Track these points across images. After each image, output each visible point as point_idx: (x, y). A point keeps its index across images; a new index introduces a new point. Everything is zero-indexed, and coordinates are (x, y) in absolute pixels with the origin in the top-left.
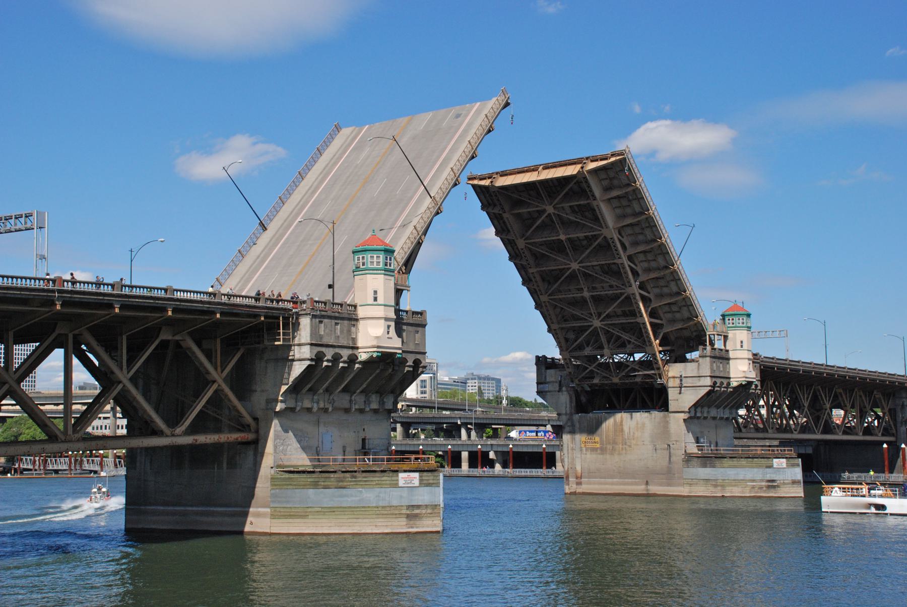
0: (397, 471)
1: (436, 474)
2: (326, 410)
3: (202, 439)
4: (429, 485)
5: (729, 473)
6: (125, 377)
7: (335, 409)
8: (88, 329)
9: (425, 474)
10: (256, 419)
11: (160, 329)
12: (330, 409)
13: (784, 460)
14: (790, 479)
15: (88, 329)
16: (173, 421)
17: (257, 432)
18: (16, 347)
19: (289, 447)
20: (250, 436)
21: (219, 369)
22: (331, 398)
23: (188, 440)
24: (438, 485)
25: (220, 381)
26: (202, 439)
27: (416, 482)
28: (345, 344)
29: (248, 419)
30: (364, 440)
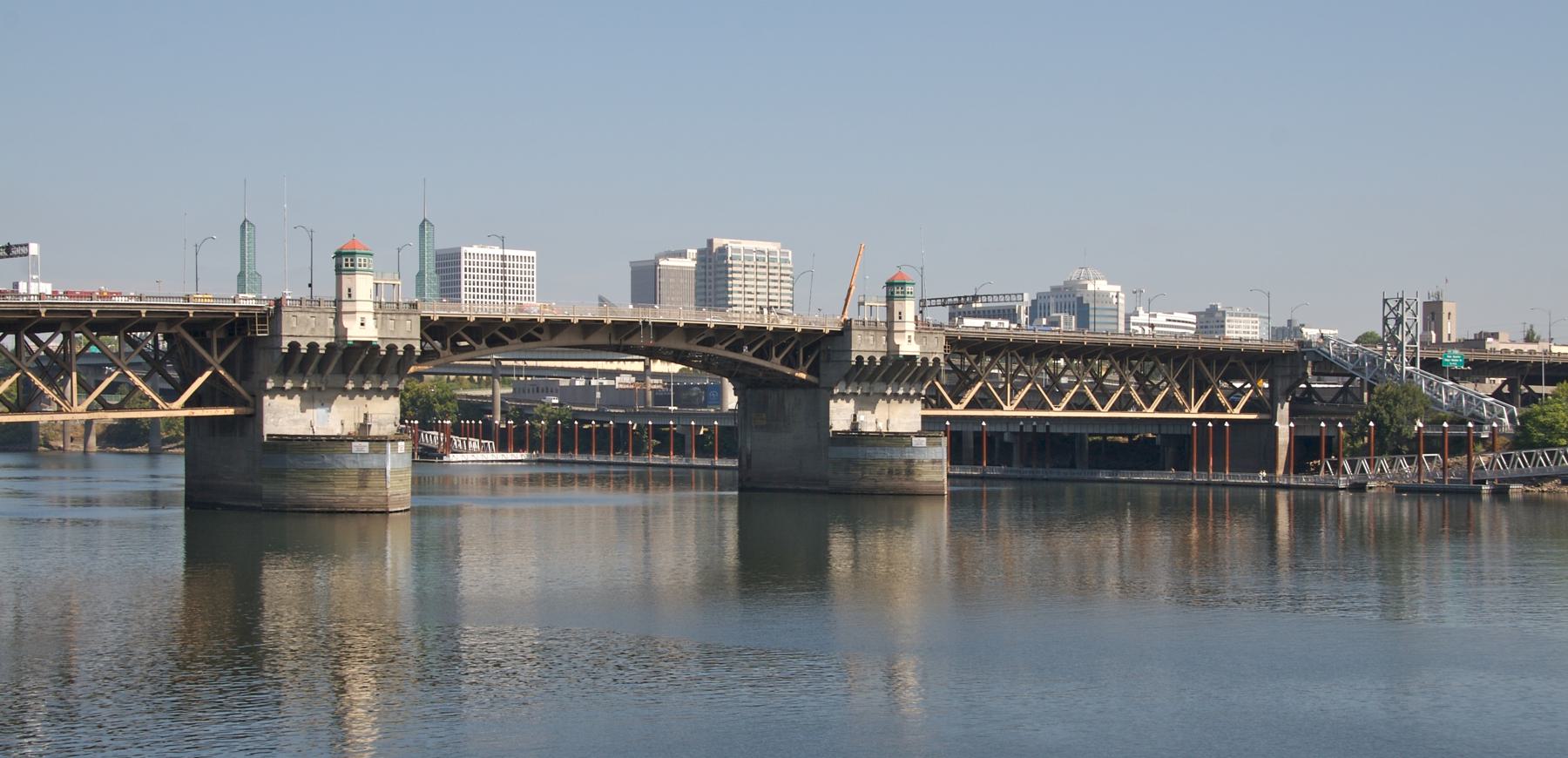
0: (353, 441)
1: (384, 443)
2: (319, 389)
3: (199, 412)
4: (377, 452)
5: (868, 451)
6: (123, 364)
7: (328, 388)
8: (86, 325)
9: (374, 443)
10: (253, 396)
11: (156, 324)
12: (323, 388)
13: (924, 439)
14: (930, 458)
15: (86, 325)
16: (169, 396)
17: (255, 407)
18: (44, 341)
19: (281, 420)
20: (248, 411)
21: (216, 355)
22: (324, 378)
23: (188, 413)
24: (385, 452)
25: (216, 365)
26: (199, 412)
27: (366, 450)
28: (322, 334)
29: (248, 397)
30: (366, 415)
